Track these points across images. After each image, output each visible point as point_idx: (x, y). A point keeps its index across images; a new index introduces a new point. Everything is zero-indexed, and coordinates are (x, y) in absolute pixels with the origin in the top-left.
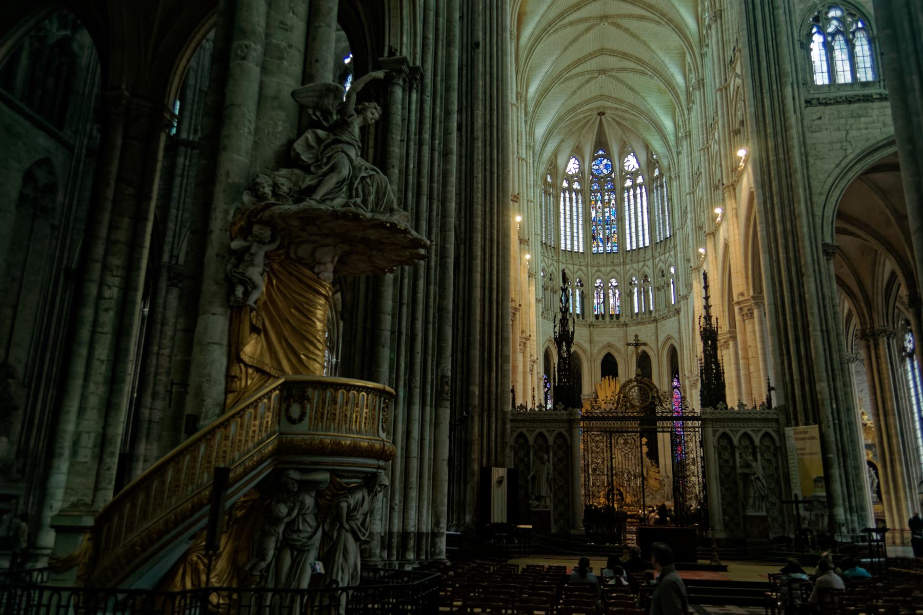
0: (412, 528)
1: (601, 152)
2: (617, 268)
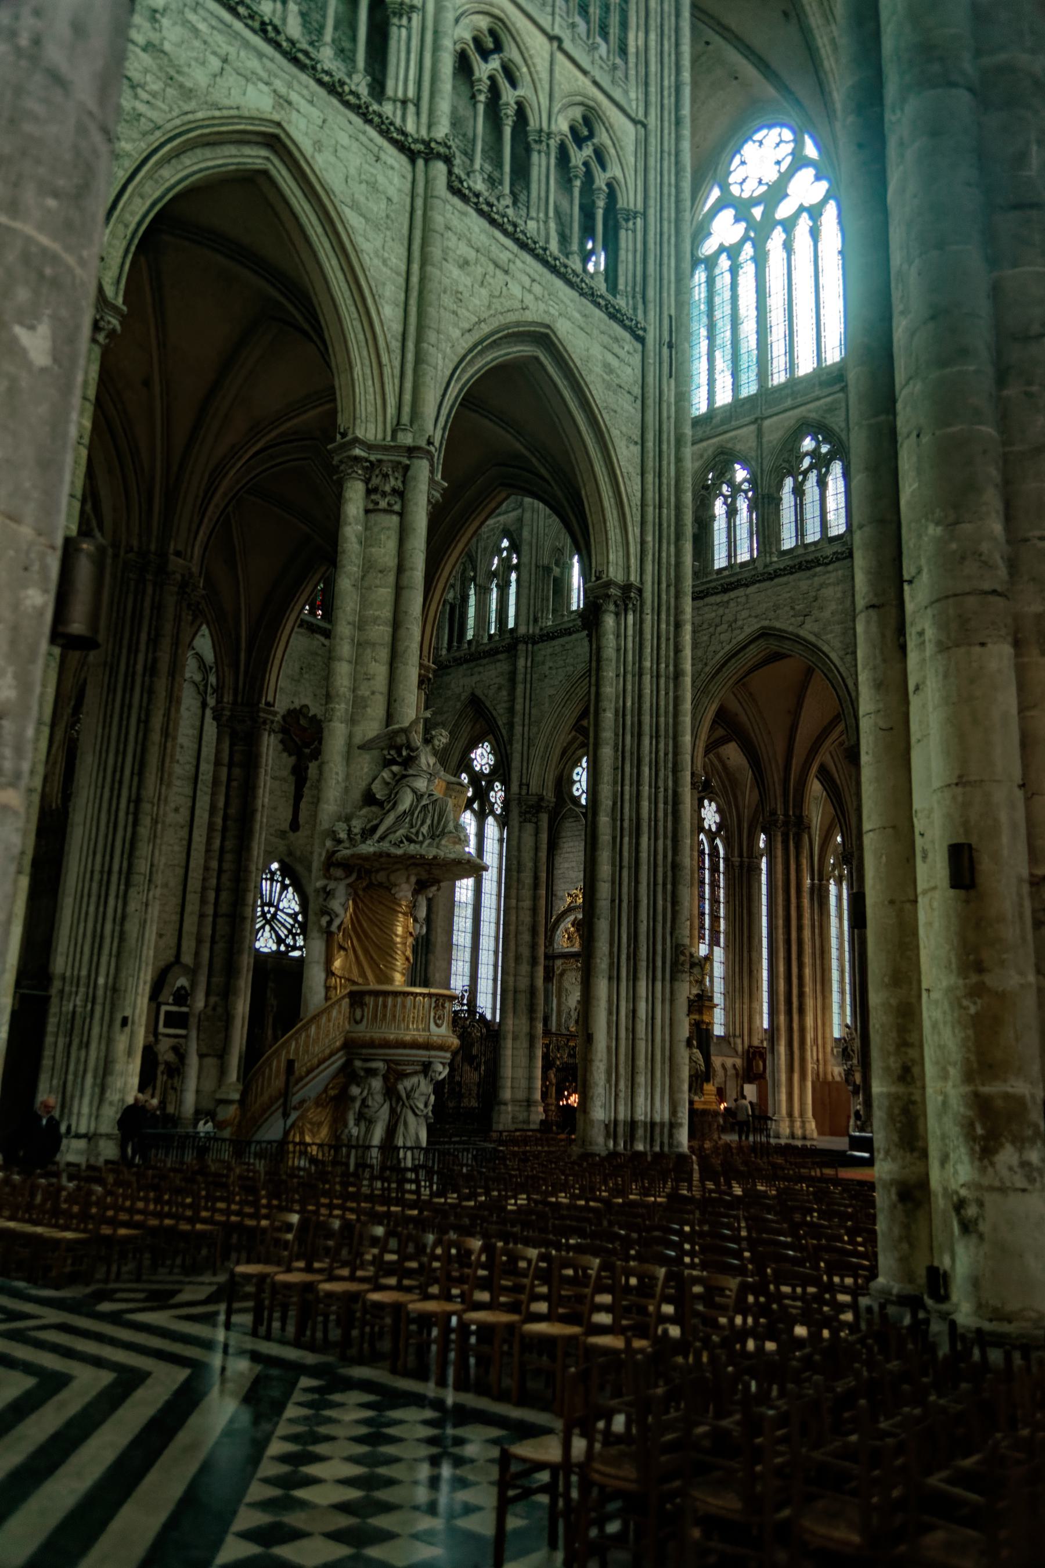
0: (640, 1117)
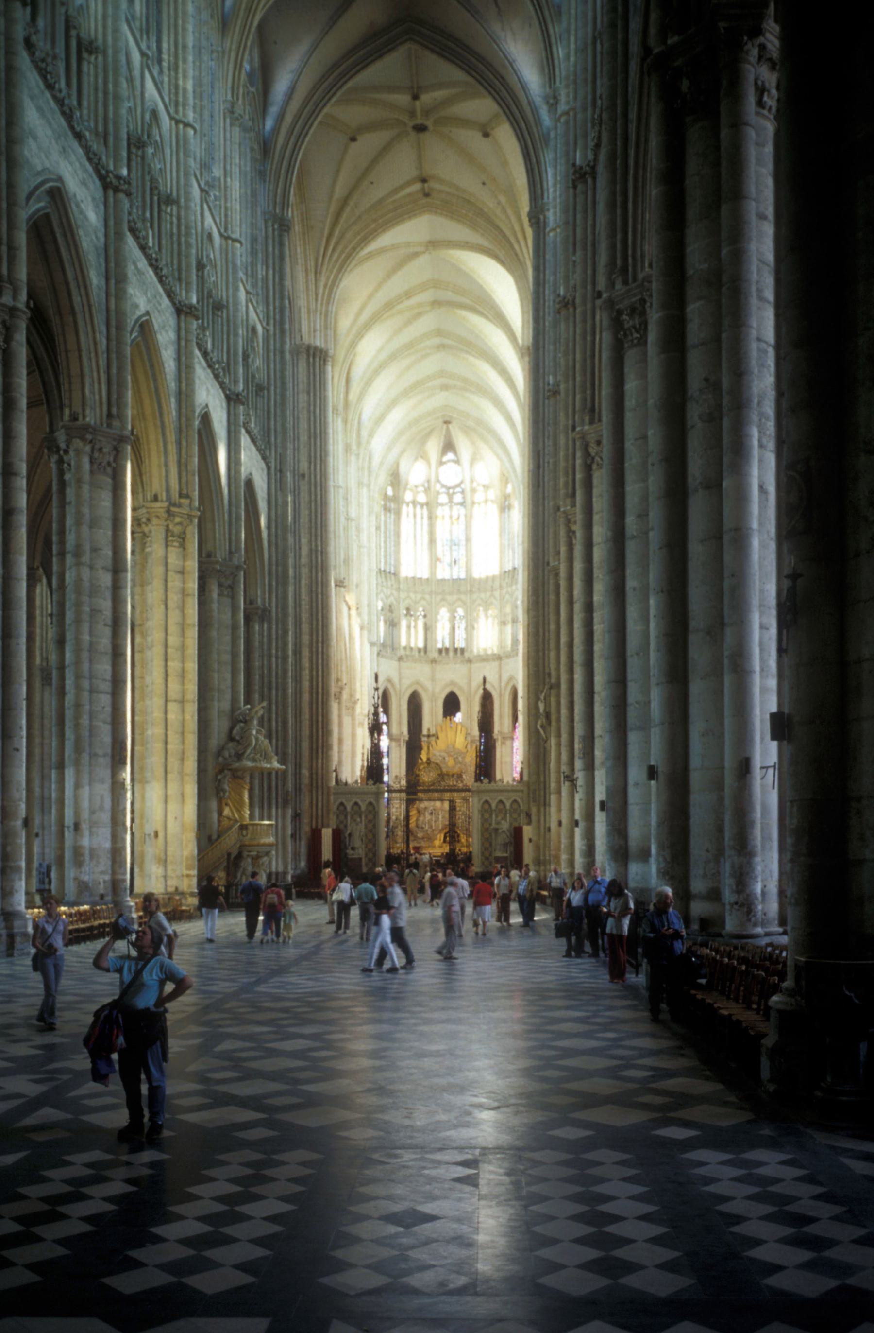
1: (450, 456)
2: (463, 597)
